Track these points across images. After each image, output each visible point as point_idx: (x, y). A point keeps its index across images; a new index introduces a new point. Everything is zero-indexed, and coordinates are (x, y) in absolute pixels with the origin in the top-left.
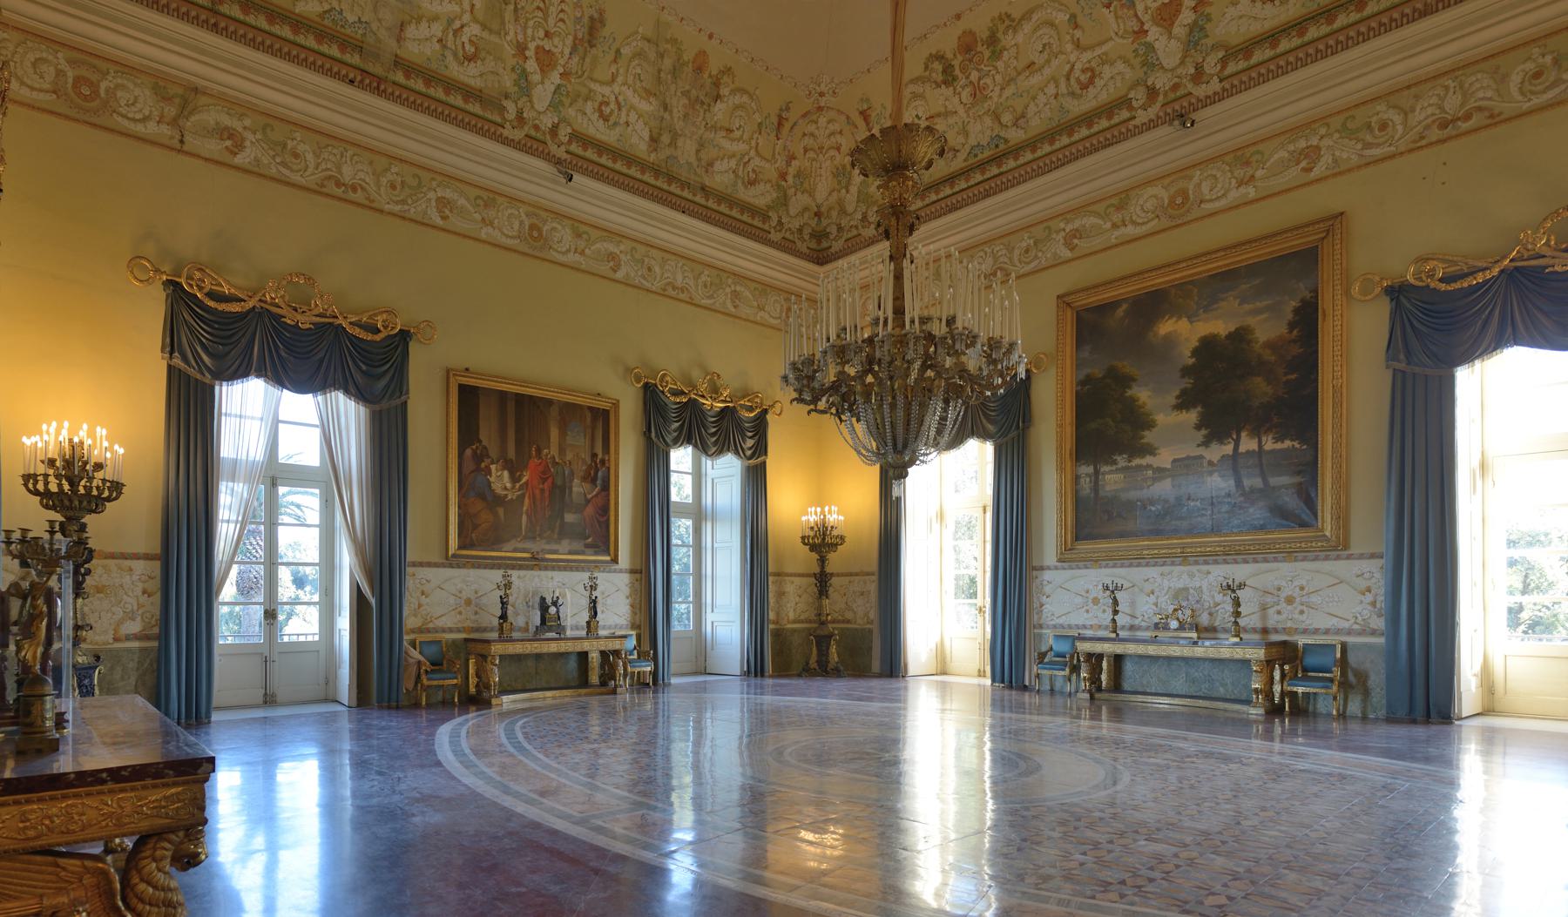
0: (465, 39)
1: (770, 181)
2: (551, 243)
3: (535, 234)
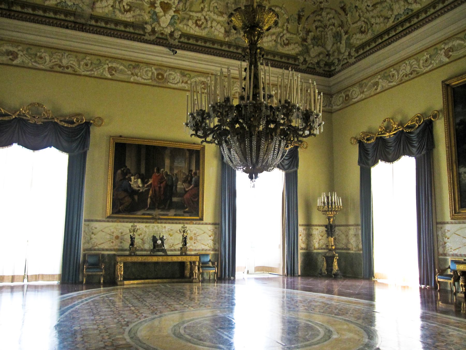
0: (124, 4)
2: (169, 80)
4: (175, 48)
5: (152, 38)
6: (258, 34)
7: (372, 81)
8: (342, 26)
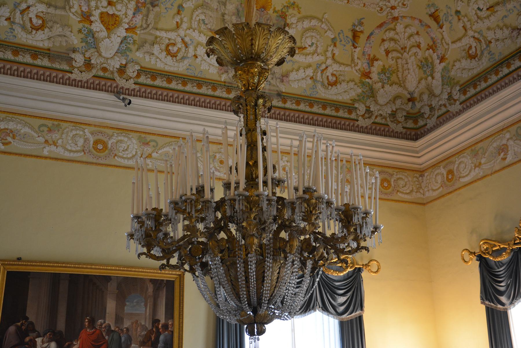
0: (32, 15)
1: (353, 81)
2: (116, 152)
3: (100, 147)
4: (128, 95)
5: (86, 76)
6: (259, 72)
7: (495, 145)
8: (433, 47)
